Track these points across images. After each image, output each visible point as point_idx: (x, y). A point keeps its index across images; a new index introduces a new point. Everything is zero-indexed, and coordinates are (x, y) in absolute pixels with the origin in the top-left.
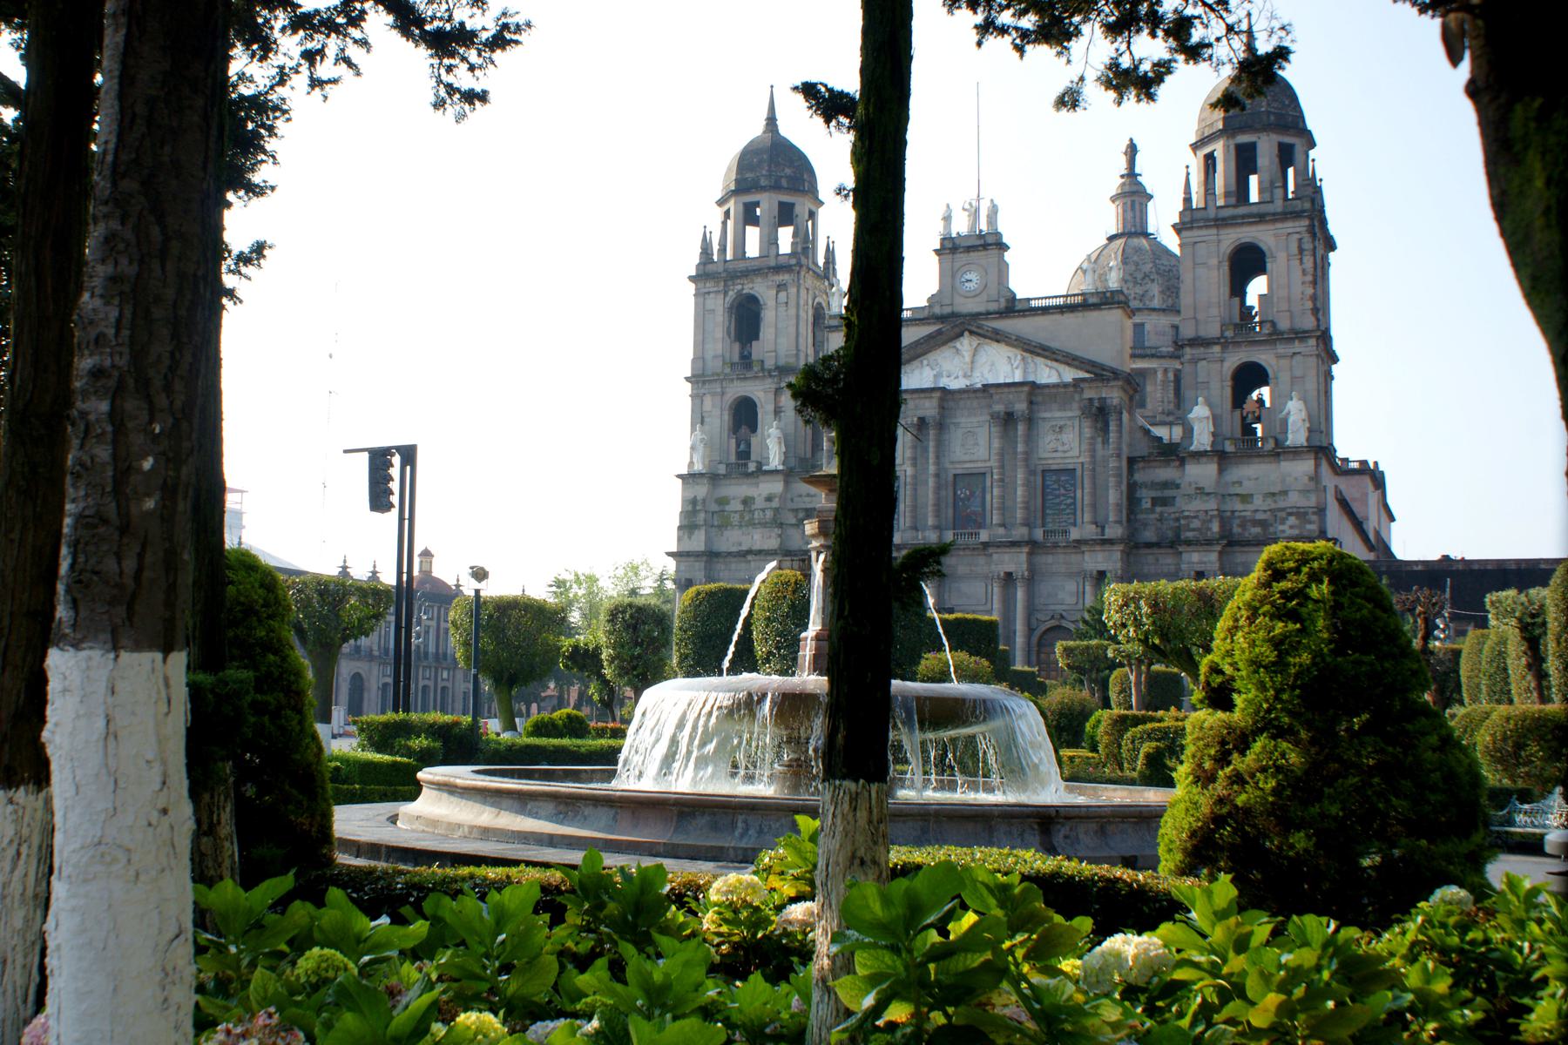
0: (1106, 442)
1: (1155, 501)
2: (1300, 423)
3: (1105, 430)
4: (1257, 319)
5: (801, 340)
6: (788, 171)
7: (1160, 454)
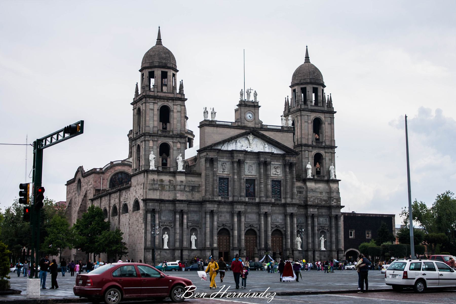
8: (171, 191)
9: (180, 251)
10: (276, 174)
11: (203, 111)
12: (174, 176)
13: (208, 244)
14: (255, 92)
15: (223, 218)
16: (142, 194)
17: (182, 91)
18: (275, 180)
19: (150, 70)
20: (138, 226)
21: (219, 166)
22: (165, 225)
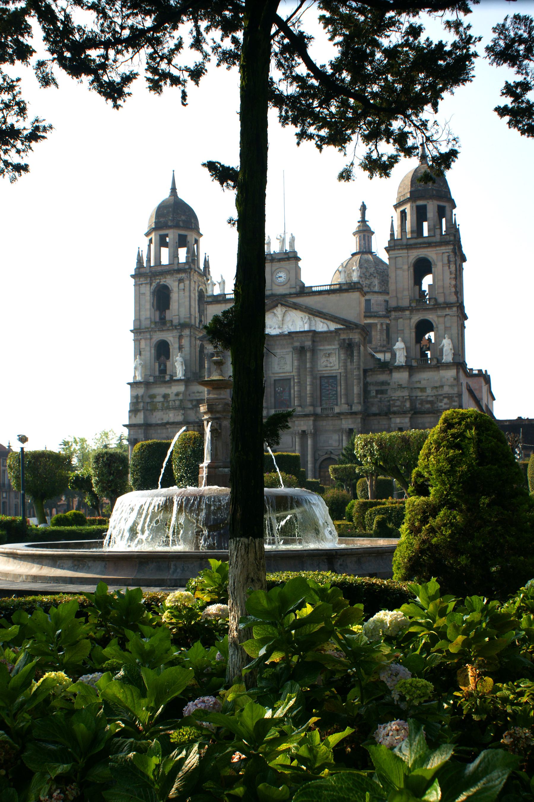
0: (352, 361)
1: (377, 392)
2: (449, 351)
3: (351, 355)
4: (427, 297)
5: (192, 309)
6: (183, 218)
7: (380, 368)
10: (327, 367)
18: (326, 375)
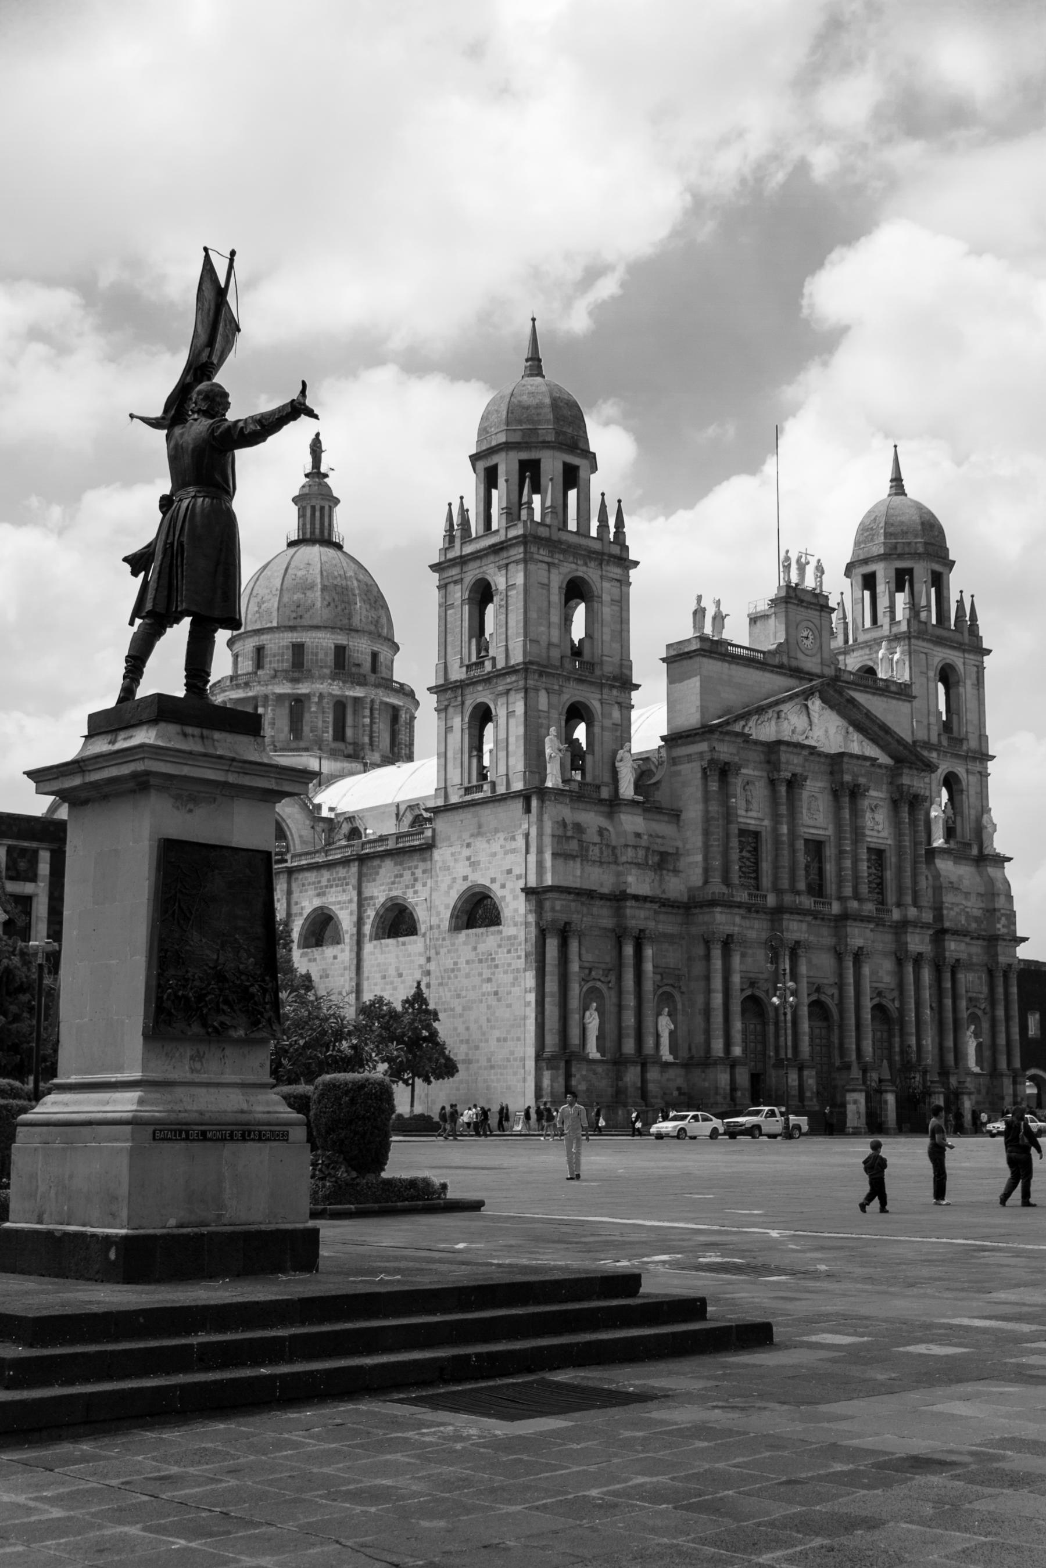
8: (605, 866)
9: (639, 1068)
11: (693, 606)
12: (610, 815)
13: (718, 1046)
14: (819, 561)
15: (750, 960)
16: (519, 870)
17: (621, 537)
19: (525, 455)
20: (489, 980)
21: (739, 790)
22: (594, 979)
